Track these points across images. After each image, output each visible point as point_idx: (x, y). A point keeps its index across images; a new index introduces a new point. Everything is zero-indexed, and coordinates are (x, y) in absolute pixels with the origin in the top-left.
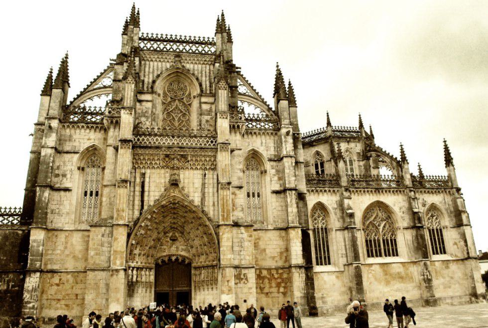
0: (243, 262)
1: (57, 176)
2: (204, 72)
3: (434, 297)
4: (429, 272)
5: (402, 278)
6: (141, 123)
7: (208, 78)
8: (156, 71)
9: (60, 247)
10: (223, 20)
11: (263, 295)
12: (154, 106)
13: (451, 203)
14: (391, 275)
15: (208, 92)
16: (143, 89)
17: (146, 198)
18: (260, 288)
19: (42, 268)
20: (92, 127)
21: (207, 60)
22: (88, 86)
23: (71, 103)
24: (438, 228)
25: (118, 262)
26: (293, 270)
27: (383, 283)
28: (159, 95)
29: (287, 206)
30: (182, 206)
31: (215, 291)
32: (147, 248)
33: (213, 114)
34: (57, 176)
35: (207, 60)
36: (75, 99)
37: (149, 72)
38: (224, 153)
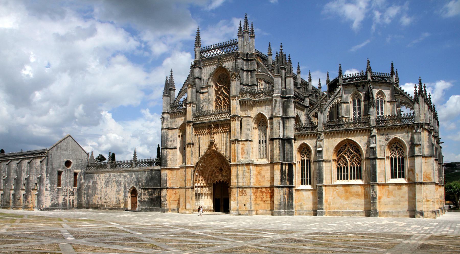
0: (244, 184)
1: (171, 141)
3: (376, 210)
4: (375, 192)
5: (358, 195)
11: (262, 202)
14: (350, 193)
17: (201, 151)
19: (168, 186)
22: (182, 87)
23: (176, 99)
25: (189, 184)
26: (275, 189)
27: (343, 198)
32: (207, 176)
36: (177, 96)
38: (234, 122)
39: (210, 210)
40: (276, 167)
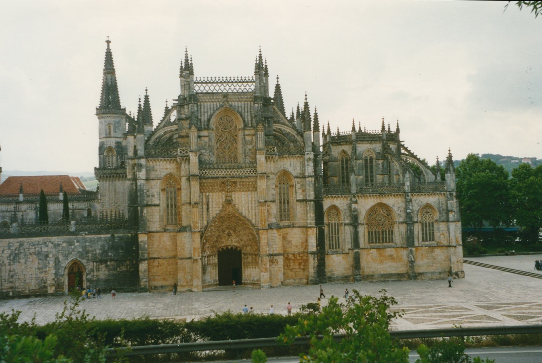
0: (275, 252)
1: (148, 196)
2: (246, 108)
5: (393, 259)
6: (202, 154)
7: (249, 114)
8: (209, 110)
9: (156, 243)
10: (260, 57)
12: (210, 140)
13: (444, 203)
15: (250, 125)
16: (201, 127)
18: (287, 266)
20: (168, 160)
21: (249, 97)
24: (431, 222)
28: (213, 130)
29: (307, 212)
30: (234, 216)
31: (257, 269)
33: (254, 143)
34: (148, 196)
35: (249, 97)
37: (204, 112)
39: (216, 285)
40: (310, 231)
